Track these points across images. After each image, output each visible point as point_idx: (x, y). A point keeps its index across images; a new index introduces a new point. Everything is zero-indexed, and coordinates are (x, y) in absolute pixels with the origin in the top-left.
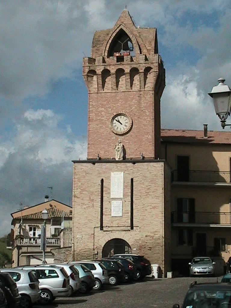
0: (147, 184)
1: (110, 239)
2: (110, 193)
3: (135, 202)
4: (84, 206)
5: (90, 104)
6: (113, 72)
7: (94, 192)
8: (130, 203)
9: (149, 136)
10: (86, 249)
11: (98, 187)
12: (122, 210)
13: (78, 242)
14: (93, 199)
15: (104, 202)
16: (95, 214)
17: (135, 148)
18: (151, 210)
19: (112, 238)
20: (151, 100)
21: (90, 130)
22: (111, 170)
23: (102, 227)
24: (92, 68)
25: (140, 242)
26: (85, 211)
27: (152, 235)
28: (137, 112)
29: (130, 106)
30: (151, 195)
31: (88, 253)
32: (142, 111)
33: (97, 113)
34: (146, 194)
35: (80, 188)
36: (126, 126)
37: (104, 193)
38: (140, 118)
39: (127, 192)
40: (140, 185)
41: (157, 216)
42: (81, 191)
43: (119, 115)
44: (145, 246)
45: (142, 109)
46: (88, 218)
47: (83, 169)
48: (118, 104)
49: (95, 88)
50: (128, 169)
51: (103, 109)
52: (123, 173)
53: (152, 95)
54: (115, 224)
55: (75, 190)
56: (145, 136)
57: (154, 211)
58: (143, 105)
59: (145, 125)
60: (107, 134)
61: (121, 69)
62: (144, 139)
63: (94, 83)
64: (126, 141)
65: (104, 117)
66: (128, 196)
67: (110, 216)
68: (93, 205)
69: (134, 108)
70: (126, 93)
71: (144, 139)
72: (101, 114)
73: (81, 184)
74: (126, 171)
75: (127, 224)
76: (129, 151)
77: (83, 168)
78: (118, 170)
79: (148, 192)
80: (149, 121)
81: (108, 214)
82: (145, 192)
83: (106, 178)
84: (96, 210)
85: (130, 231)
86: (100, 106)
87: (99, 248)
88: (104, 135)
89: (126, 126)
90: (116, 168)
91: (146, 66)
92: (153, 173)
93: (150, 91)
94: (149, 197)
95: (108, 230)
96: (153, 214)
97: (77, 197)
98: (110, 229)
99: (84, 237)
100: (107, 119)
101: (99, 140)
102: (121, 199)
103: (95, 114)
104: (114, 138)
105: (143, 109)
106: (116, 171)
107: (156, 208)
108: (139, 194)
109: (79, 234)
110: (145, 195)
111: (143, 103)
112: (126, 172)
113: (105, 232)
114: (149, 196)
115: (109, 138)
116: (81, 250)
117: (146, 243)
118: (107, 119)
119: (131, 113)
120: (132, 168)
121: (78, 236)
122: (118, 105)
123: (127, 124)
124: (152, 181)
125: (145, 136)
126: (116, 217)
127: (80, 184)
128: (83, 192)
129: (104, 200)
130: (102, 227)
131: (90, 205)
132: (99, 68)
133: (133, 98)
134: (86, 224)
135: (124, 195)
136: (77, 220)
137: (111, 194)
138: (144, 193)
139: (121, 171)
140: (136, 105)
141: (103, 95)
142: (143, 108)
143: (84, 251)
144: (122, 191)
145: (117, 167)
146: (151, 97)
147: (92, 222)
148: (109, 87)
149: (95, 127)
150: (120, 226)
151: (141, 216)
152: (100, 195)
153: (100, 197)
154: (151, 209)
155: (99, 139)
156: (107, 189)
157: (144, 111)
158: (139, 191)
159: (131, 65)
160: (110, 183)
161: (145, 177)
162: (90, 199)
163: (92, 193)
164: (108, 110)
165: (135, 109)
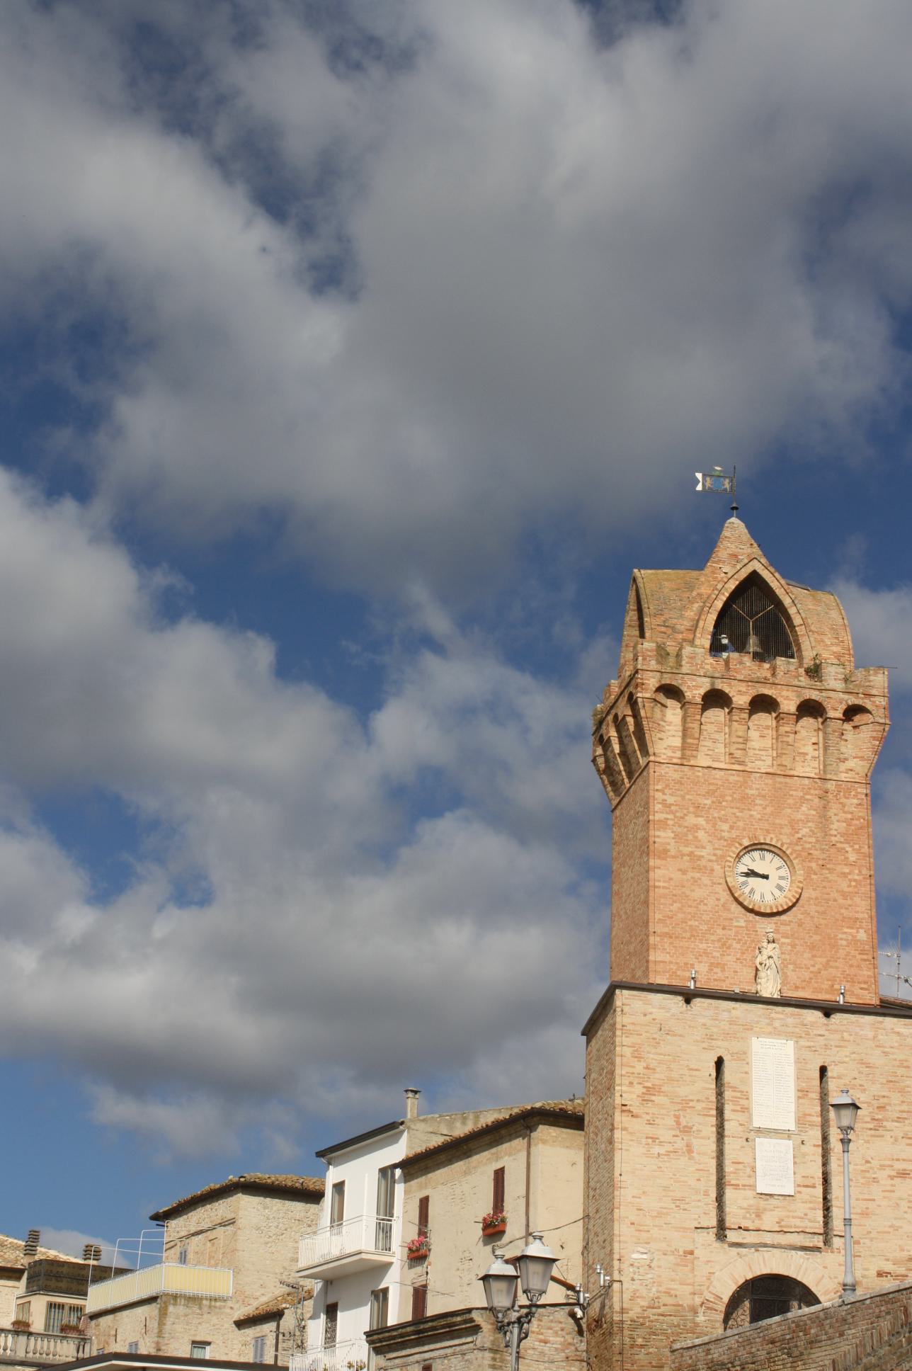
1: (750, 1276)
2: (746, 1110)
4: (657, 1149)
5: (656, 796)
6: (741, 702)
7: (692, 1101)
8: (820, 1150)
9: (858, 932)
10: (664, 1305)
12: (795, 1173)
13: (636, 1277)
14: (689, 1125)
15: (726, 1140)
16: (699, 1180)
20: (860, 814)
21: (659, 887)
22: (748, 1028)
24: (667, 680)
26: (661, 1164)
27: (902, 1271)
28: (818, 846)
29: (793, 824)
30: (892, 1130)
31: (676, 1320)
32: (833, 845)
33: (679, 830)
34: (871, 1126)
35: (641, 1081)
36: (780, 888)
37: (728, 1109)
38: (828, 869)
39: (807, 1111)
42: (643, 1093)
43: (759, 847)
45: (833, 839)
46: (671, 1194)
47: (654, 1016)
48: (752, 813)
49: (673, 749)
51: (701, 821)
52: (791, 1043)
53: (863, 796)
54: (769, 1221)
55: (624, 1088)
56: (846, 930)
58: (837, 826)
59: (845, 895)
60: (718, 906)
61: (770, 697)
62: (841, 939)
63: (669, 731)
64: (783, 940)
65: (704, 847)
66: (812, 1125)
67: (750, 1193)
68: (688, 1145)
69: (805, 831)
71: (841, 939)
72: (696, 837)
73: (647, 1068)
74: (801, 1037)
75: (811, 1224)
76: (793, 973)
77: (650, 1010)
78: (776, 1033)
80: (855, 880)
82: (868, 1119)
83: (732, 1054)
84: (701, 1167)
85: (817, 1249)
86: (691, 809)
87: (711, 1305)
88: (705, 908)
89: (780, 888)
90: (768, 1024)
91: (850, 703)
92: (893, 1054)
93: (856, 785)
94: (883, 1136)
95: (745, 1241)
96: (900, 1199)
97: (629, 1111)
98: (749, 1238)
99: (659, 1259)
100: (715, 855)
101: (689, 923)
102: (787, 1134)
103: (672, 835)
104: (742, 923)
105: (836, 839)
106: (769, 1034)
110: (871, 1129)
111: (834, 818)
112: (803, 1043)
113: (735, 1250)
115: (727, 923)
116: (648, 1308)
118: (714, 858)
119: (799, 848)
120: (822, 1033)
121: (635, 1256)
122: (751, 816)
123: (782, 883)
124: (891, 1081)
125: (846, 930)
126: (771, 1195)
127: (639, 1067)
128: (653, 1098)
129: (726, 1133)
131: (680, 1144)
132: (694, 683)
133: (803, 800)
134: (667, 1214)
135: (801, 1120)
136: (633, 1197)
137: (755, 1112)
138: (866, 1122)
139: (788, 1036)
140: (810, 824)
141: (700, 774)
142: (835, 836)
143: (659, 1311)
144: (792, 1107)
145: (772, 1019)
146: (860, 804)
147: (686, 1206)
148: (716, 750)
149: (672, 876)
150: (785, 1230)
152: (714, 1112)
153: (713, 1120)
154: (892, 1178)
155: (690, 920)
156: (739, 1095)
157: (839, 845)
159: (799, 689)
160: (746, 1073)
161: (867, 1067)
162: (678, 1123)
163: (685, 1104)
164: (717, 827)
165: (810, 836)
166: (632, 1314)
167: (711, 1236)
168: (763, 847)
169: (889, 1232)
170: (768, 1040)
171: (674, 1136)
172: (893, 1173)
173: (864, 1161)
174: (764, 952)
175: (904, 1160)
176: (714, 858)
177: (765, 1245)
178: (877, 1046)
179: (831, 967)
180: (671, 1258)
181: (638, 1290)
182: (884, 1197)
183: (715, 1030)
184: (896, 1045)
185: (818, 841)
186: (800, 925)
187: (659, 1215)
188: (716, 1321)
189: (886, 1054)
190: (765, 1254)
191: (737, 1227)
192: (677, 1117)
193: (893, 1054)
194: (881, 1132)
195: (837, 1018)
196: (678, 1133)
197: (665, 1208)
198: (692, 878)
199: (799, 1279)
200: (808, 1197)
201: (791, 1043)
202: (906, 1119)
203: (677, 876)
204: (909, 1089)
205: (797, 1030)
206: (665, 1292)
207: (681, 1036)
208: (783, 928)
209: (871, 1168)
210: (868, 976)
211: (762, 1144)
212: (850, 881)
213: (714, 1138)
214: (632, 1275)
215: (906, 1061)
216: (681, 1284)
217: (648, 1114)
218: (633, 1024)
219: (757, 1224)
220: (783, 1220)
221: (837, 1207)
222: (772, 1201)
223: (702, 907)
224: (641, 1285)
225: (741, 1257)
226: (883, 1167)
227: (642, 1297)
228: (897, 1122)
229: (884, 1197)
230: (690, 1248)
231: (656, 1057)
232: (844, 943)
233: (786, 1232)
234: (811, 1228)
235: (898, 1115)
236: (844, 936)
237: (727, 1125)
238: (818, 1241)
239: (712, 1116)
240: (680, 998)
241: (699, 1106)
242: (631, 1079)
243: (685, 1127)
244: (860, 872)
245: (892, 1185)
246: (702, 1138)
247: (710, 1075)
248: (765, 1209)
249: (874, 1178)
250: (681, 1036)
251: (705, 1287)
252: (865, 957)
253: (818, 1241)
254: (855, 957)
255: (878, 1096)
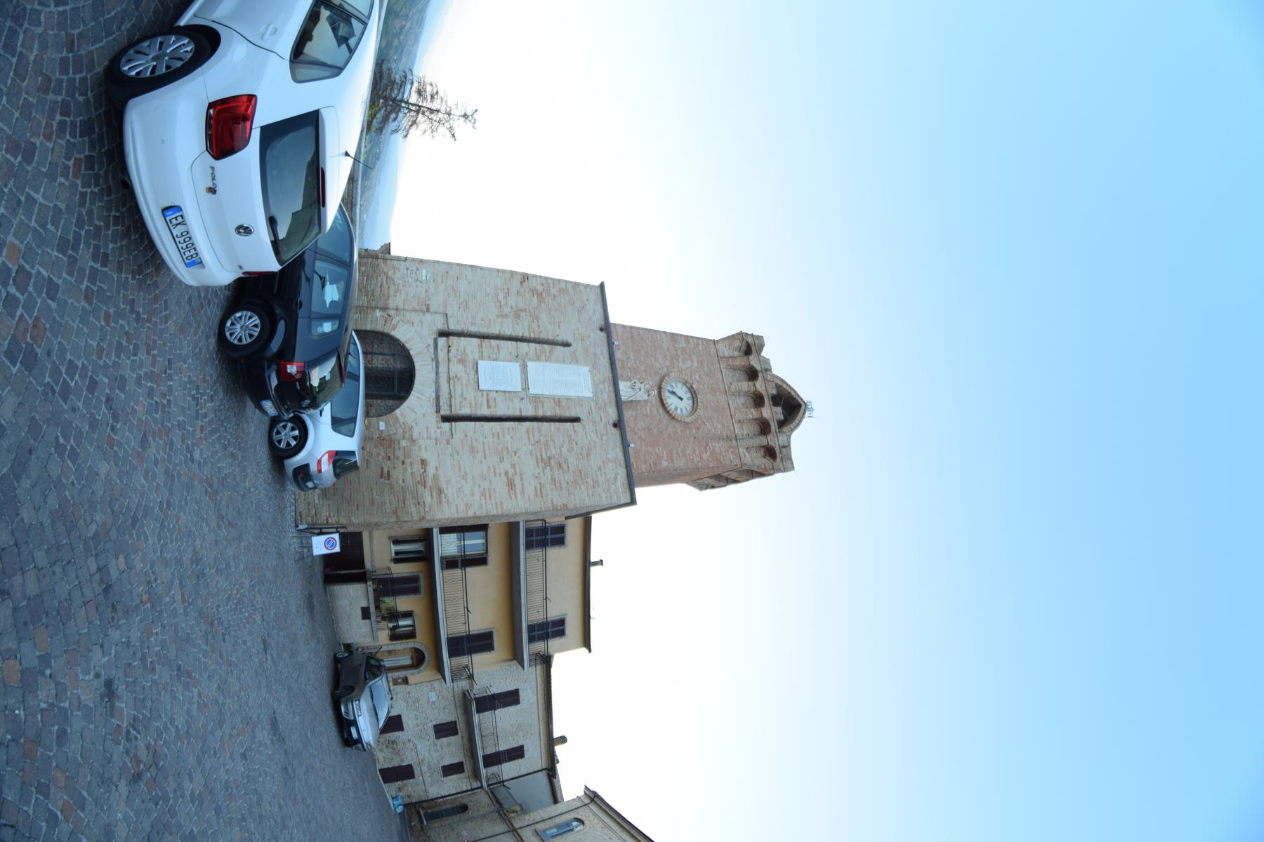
0: (572, 460)
1: (412, 353)
2: (538, 358)
3: (520, 427)
4: (501, 296)
7: (538, 322)
9: (666, 461)
10: (389, 287)
11: (550, 334)
12: (497, 391)
13: (409, 271)
15: (514, 343)
16: (482, 320)
17: (638, 429)
18: (503, 475)
19: (415, 360)
22: (594, 366)
23: (444, 334)
25: (404, 443)
27: (429, 482)
28: (704, 434)
31: (378, 293)
34: (544, 456)
37: (537, 346)
39: (545, 405)
40: (567, 441)
41: (487, 494)
43: (694, 396)
44: (392, 457)
50: (600, 408)
51: (696, 364)
52: (590, 395)
54: (457, 369)
56: (665, 452)
57: (499, 484)
59: (684, 451)
65: (684, 363)
67: (477, 355)
70: (728, 411)
73: (554, 296)
74: (596, 403)
75: (458, 403)
78: (595, 385)
79: (550, 466)
80: (693, 458)
81: (484, 352)
82: (549, 454)
84: (492, 323)
85: (438, 411)
90: (600, 380)
92: (601, 475)
94: (538, 466)
95: (439, 351)
96: (490, 481)
97: (524, 281)
98: (442, 354)
101: (642, 350)
102: (526, 387)
106: (593, 381)
107: (509, 491)
108: (542, 439)
109: (429, 275)
111: (720, 445)
112: (593, 404)
113: (432, 343)
114: (540, 466)
116: (387, 277)
117: (403, 463)
120: (603, 419)
121: (424, 272)
122: (707, 394)
123: (679, 411)
125: (665, 452)
126: (477, 372)
128: (536, 297)
129: (519, 343)
130: (444, 334)
131: (507, 310)
134: (455, 296)
135: (536, 399)
136: (466, 276)
139: (595, 393)
140: (713, 430)
144: (546, 392)
147: (462, 309)
150: (451, 381)
151: (484, 444)
152: (532, 336)
153: (527, 335)
154: (506, 474)
156: (548, 354)
158: (551, 440)
162: (521, 310)
163: (535, 317)
166: (382, 265)
167: (441, 325)
168: (695, 399)
169: (460, 471)
170: (589, 378)
171: (512, 307)
172: (510, 475)
173: (515, 450)
174: (642, 386)
175: (523, 484)
176: (680, 369)
177: (437, 367)
178: (603, 462)
179: (641, 443)
180: (423, 295)
181: (399, 271)
182: (489, 467)
183: (588, 343)
184: (608, 477)
185: (706, 434)
186: (659, 421)
187: (455, 291)
188: (376, 325)
189: (600, 469)
190: (430, 367)
191: (450, 344)
192: (525, 310)
193: (601, 475)
194: (541, 465)
195: (615, 433)
196: (515, 309)
197: (459, 295)
199: (413, 393)
200: (479, 402)
201: (590, 395)
202: (555, 485)
204: (578, 489)
205: (601, 401)
206: (398, 289)
207: (579, 320)
208: (654, 410)
209: (511, 456)
210: (641, 469)
211: (515, 367)
212: (692, 455)
213: (514, 334)
214: (410, 268)
215: (598, 486)
216: (404, 300)
217: (525, 292)
218: (580, 291)
219: (454, 360)
220: (459, 380)
221: (475, 425)
222: (472, 373)
223: (653, 359)
224: (404, 274)
225: (426, 347)
226: (513, 466)
227: (394, 273)
228: (552, 478)
229: (489, 467)
230: (432, 309)
231: (563, 302)
232: (657, 451)
233: (449, 382)
234: (455, 403)
235: (557, 479)
236: (661, 451)
237: (525, 344)
238: (444, 410)
239: (530, 334)
240: (603, 323)
241: (535, 326)
242: (545, 285)
243: (519, 315)
244: (698, 462)
245: (500, 474)
246: (513, 325)
247: (558, 335)
248: (465, 367)
249: (503, 458)
250: (579, 320)
251: (402, 318)
252: (652, 466)
253: (445, 411)
254: (651, 459)
255: (568, 463)
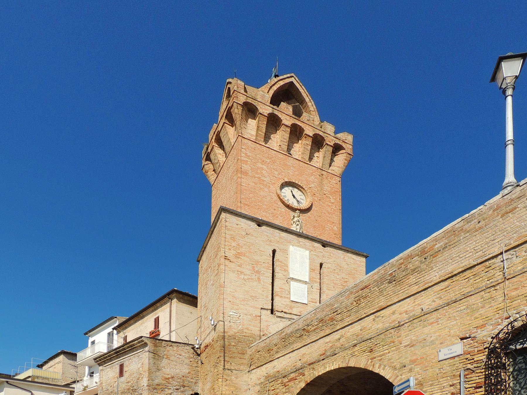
51: (265, 167)
115: (276, 208)
198: (259, 187)
203: (253, 184)
